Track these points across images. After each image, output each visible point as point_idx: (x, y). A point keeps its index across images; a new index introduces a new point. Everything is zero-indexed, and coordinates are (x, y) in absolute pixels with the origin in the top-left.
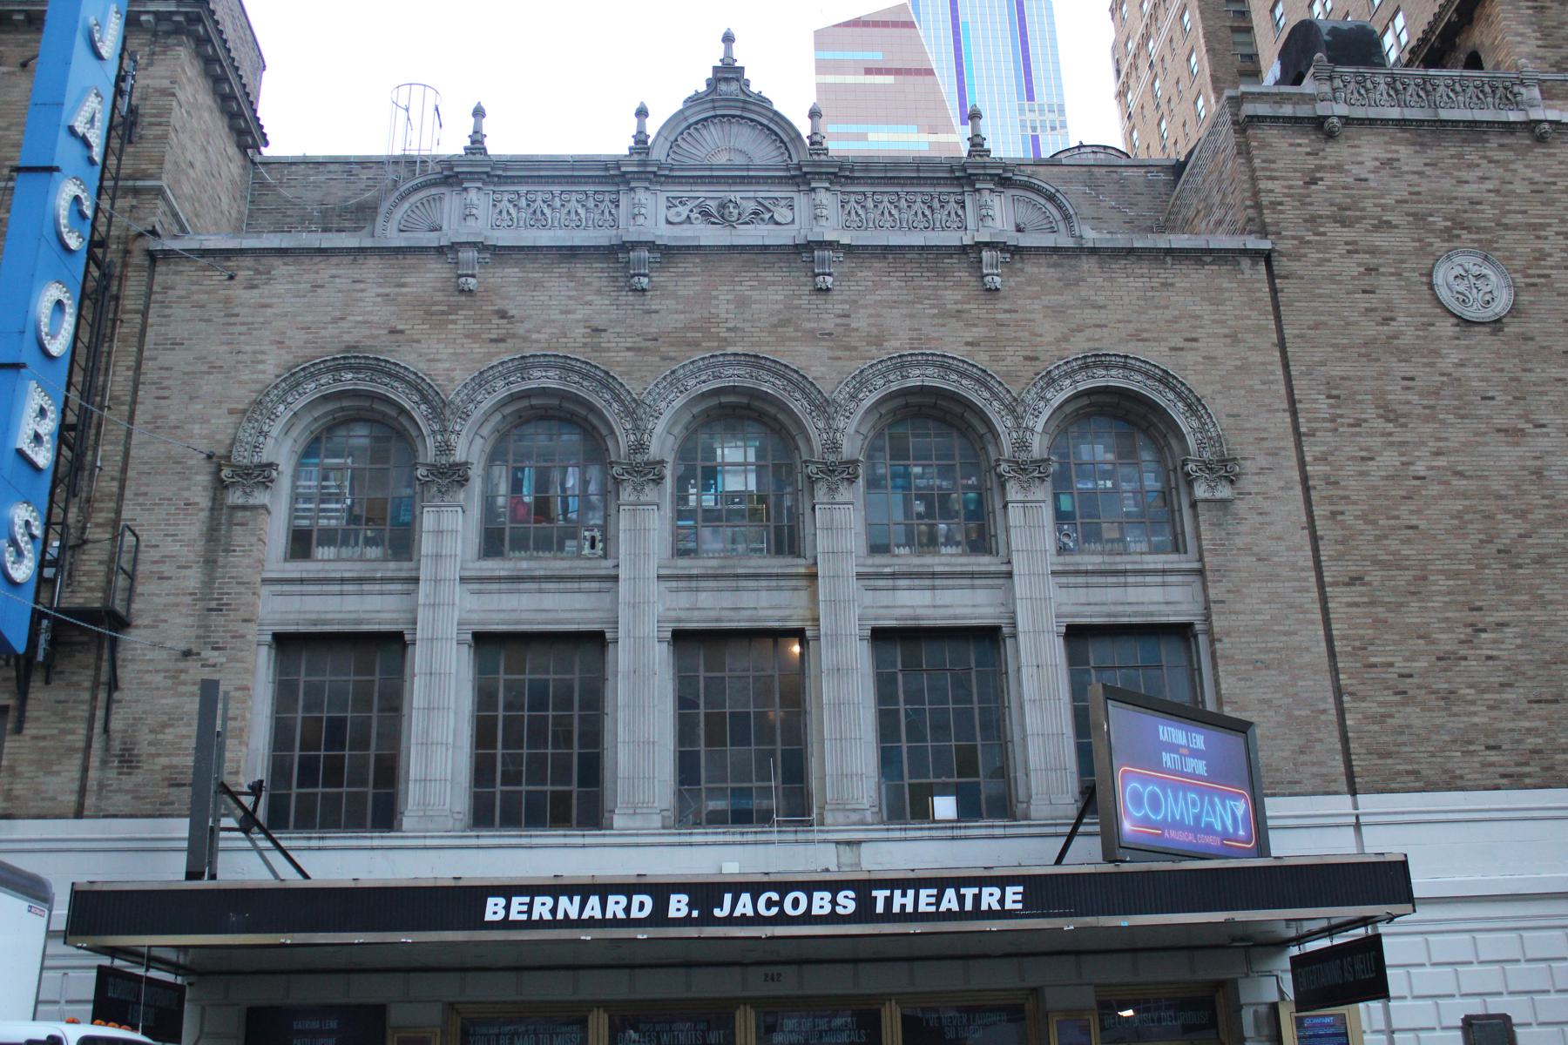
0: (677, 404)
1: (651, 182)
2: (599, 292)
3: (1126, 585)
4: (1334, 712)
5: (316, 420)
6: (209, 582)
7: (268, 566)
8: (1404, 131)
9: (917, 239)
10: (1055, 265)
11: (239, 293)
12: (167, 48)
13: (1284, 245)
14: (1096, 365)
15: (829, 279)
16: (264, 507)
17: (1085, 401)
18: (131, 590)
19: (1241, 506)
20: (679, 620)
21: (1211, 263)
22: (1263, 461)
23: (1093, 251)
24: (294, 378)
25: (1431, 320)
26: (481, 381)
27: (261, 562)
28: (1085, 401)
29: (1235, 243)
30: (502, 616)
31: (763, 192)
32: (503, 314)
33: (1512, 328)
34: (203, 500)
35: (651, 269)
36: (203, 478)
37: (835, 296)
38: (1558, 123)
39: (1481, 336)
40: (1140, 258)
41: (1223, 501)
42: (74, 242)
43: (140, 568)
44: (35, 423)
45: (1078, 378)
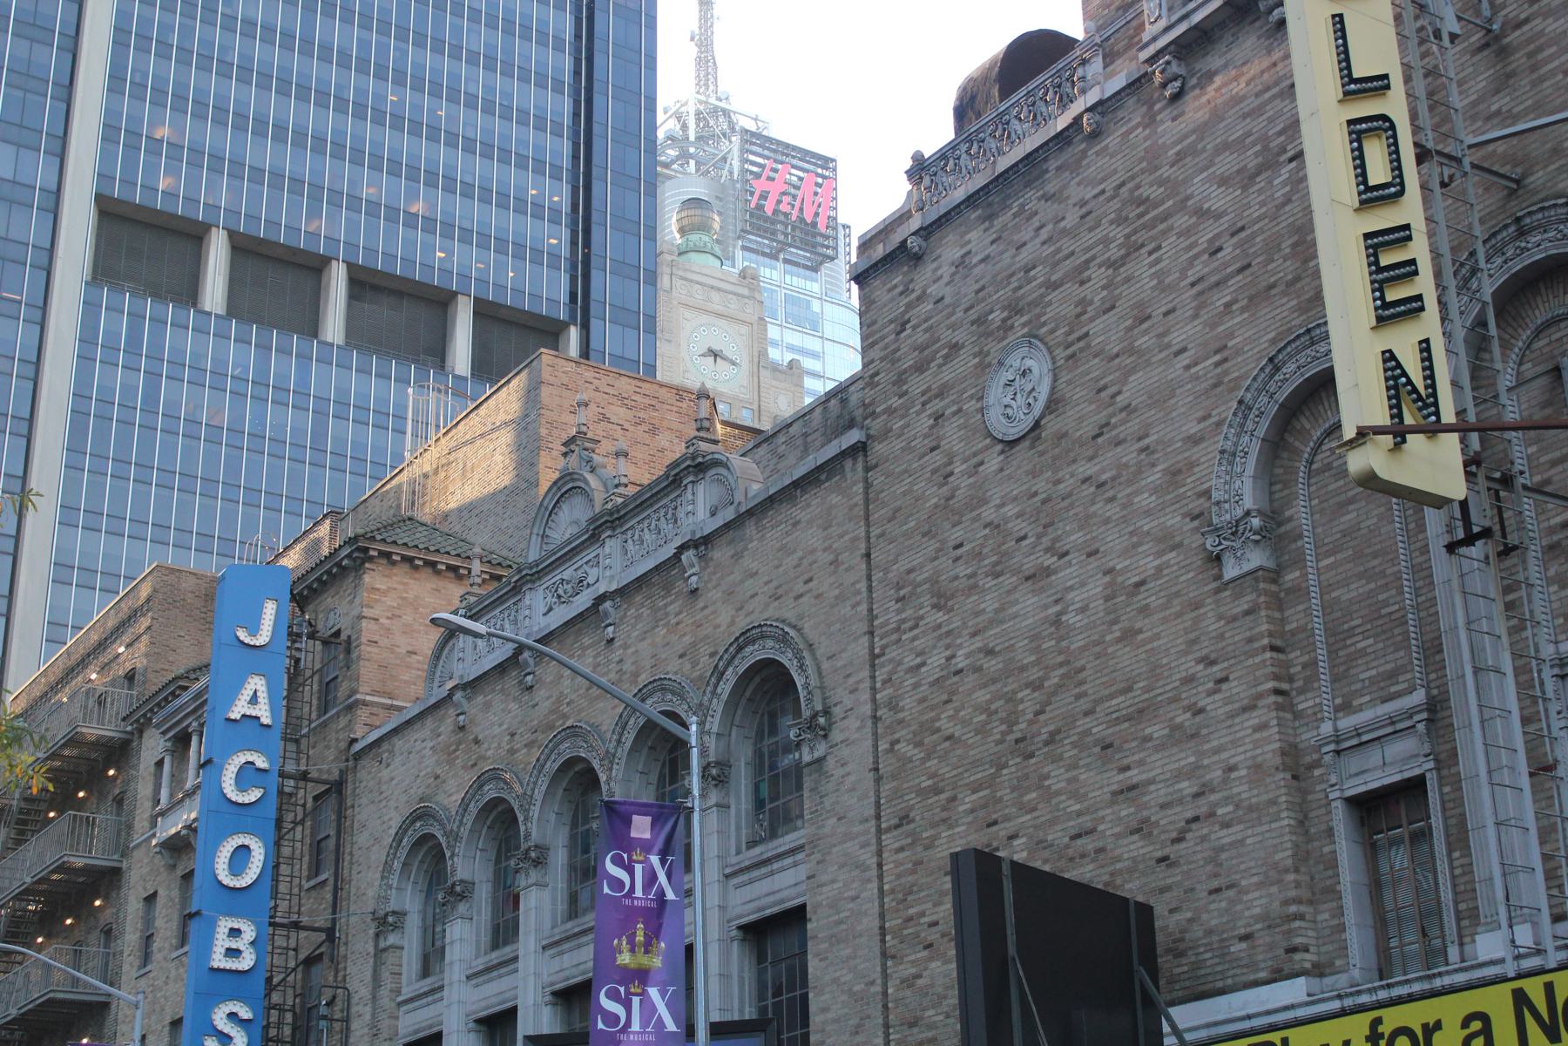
0: (544, 788)
1: (533, 582)
2: (515, 699)
3: (772, 873)
4: (879, 981)
5: (422, 862)
6: (373, 1015)
7: (404, 990)
8: (976, 207)
9: (650, 564)
10: (731, 542)
11: (385, 774)
12: (360, 578)
13: (876, 425)
14: (746, 644)
15: (611, 629)
16: (391, 946)
17: (757, 679)
18: (348, 1029)
19: (831, 762)
20: (552, 984)
21: (827, 480)
22: (848, 703)
23: (750, 513)
24: (398, 839)
25: (979, 458)
26: (464, 805)
27: (399, 992)
28: (757, 679)
29: (832, 450)
30: (483, 1004)
31: (581, 560)
32: (477, 741)
33: (1051, 426)
34: (371, 950)
35: (536, 665)
36: (372, 932)
37: (617, 644)
38: (1100, 103)
39: (1022, 452)
40: (781, 501)
41: (820, 761)
42: (253, 795)
43: (354, 1010)
44: (234, 943)
45: (736, 663)
